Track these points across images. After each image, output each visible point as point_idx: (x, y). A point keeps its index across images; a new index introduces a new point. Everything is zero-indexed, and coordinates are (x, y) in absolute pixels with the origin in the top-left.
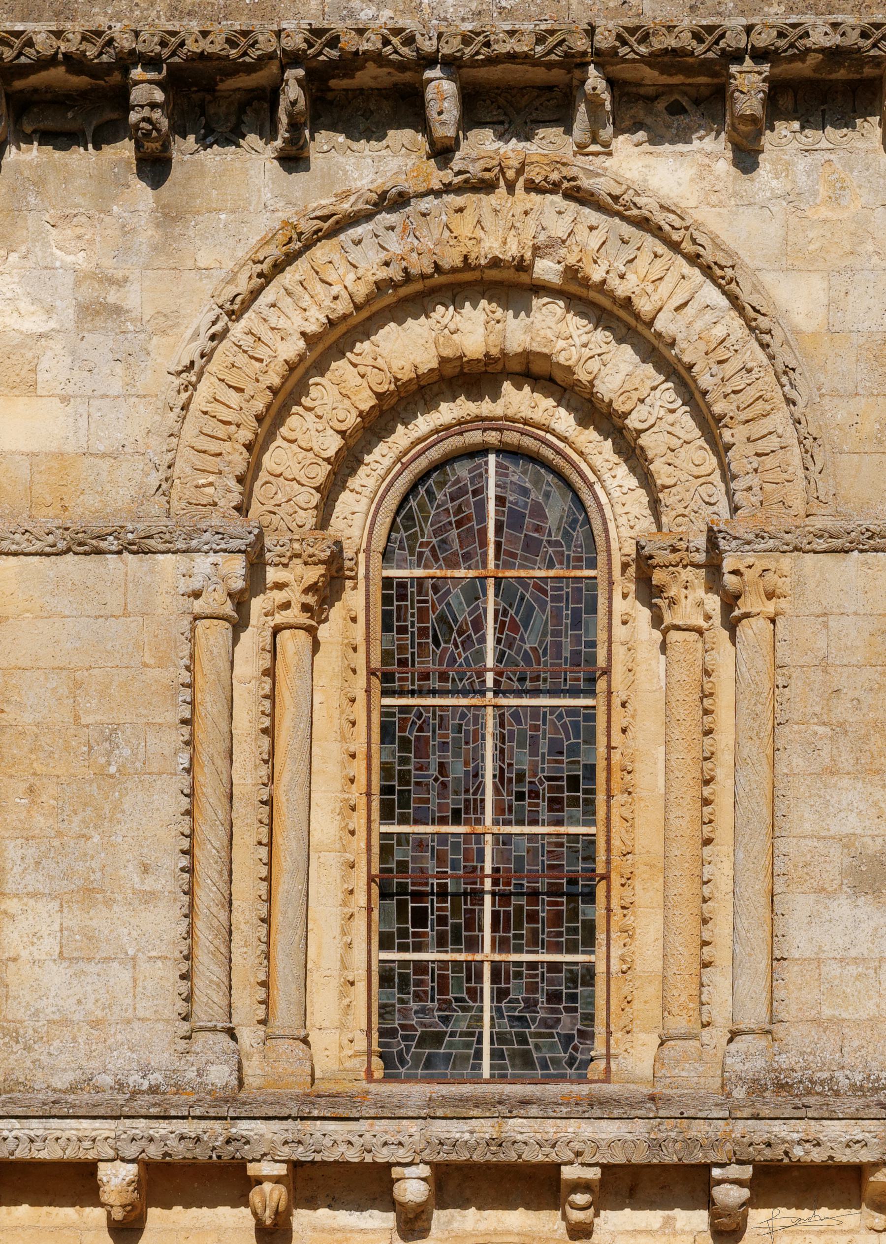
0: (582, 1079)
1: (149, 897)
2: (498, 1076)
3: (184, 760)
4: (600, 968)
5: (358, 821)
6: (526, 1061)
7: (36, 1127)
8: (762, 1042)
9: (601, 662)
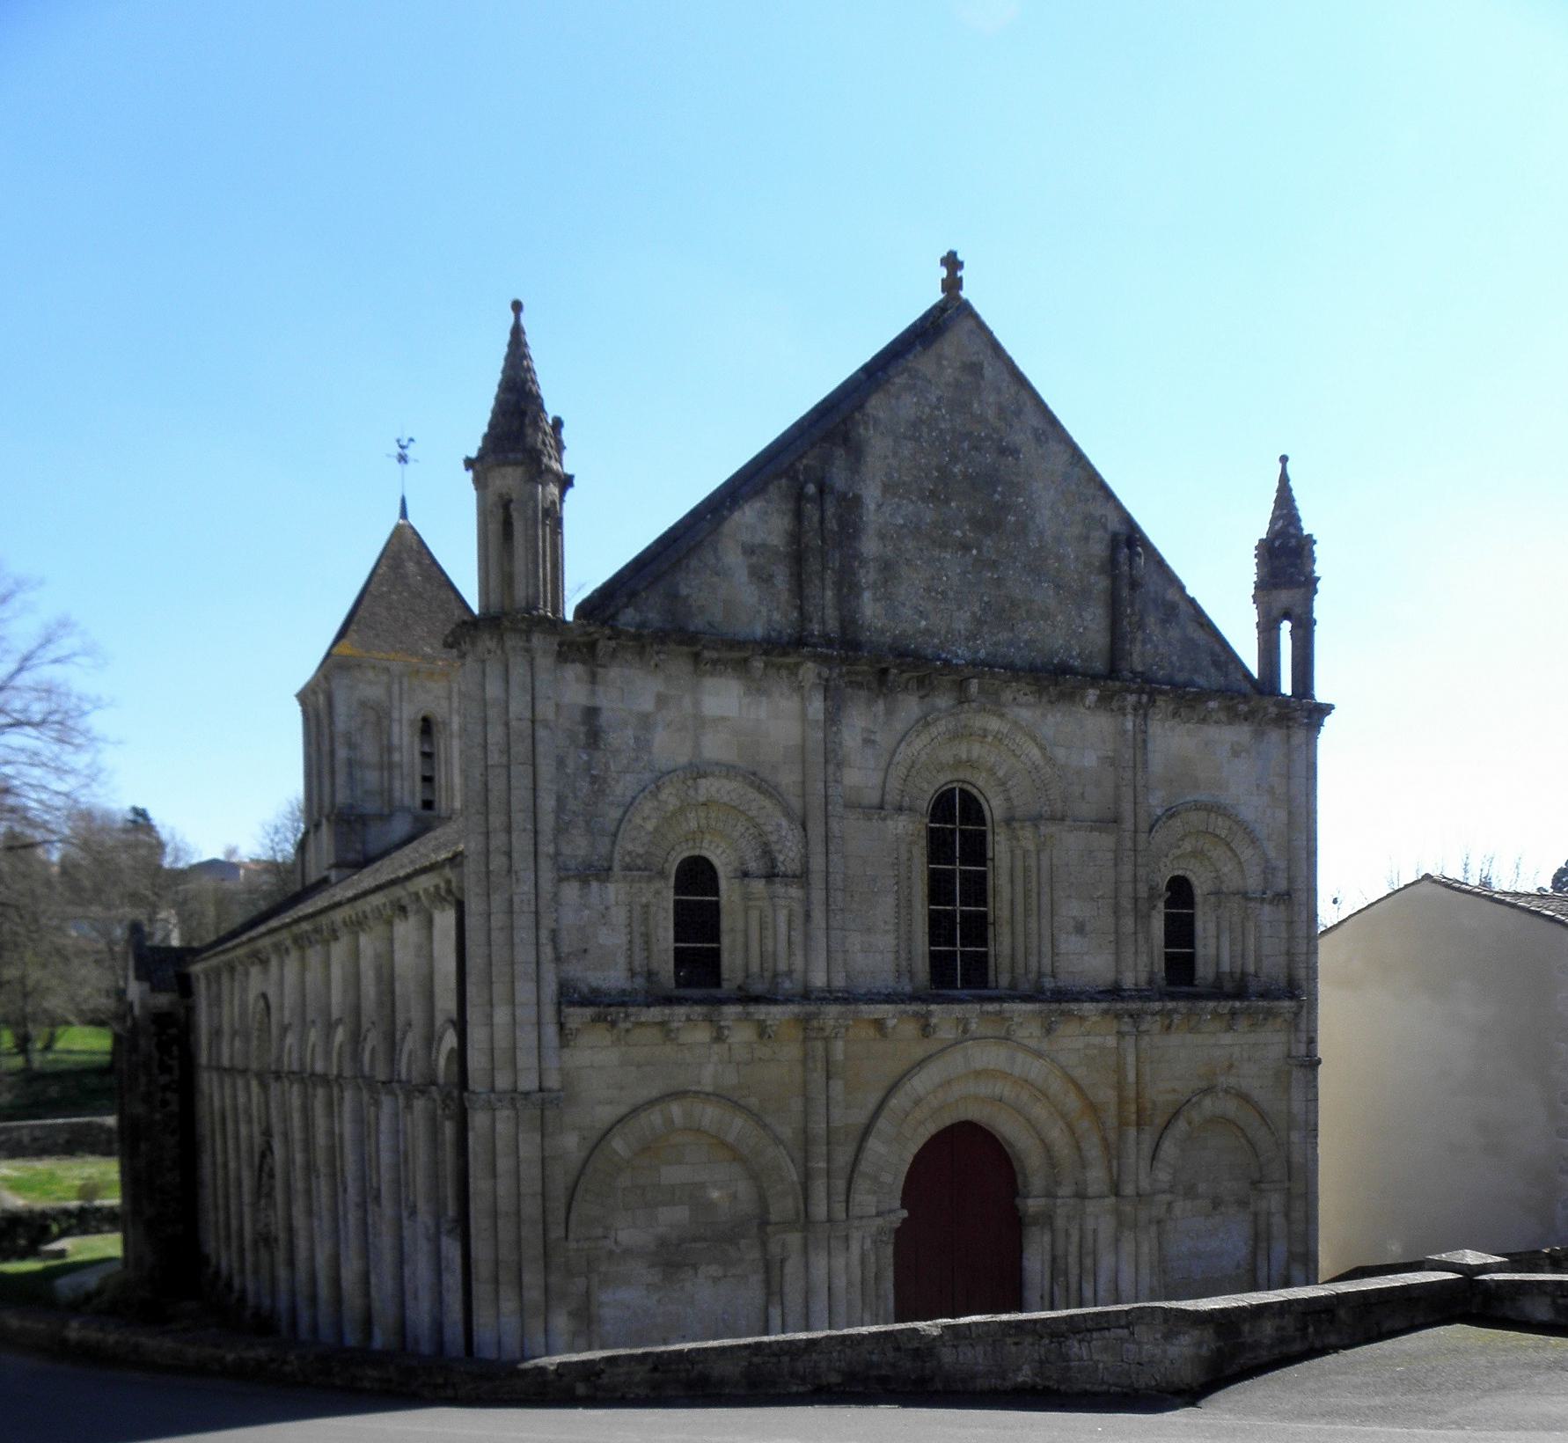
1: (887, 932)
2: (962, 988)
3: (896, 887)
4: (992, 952)
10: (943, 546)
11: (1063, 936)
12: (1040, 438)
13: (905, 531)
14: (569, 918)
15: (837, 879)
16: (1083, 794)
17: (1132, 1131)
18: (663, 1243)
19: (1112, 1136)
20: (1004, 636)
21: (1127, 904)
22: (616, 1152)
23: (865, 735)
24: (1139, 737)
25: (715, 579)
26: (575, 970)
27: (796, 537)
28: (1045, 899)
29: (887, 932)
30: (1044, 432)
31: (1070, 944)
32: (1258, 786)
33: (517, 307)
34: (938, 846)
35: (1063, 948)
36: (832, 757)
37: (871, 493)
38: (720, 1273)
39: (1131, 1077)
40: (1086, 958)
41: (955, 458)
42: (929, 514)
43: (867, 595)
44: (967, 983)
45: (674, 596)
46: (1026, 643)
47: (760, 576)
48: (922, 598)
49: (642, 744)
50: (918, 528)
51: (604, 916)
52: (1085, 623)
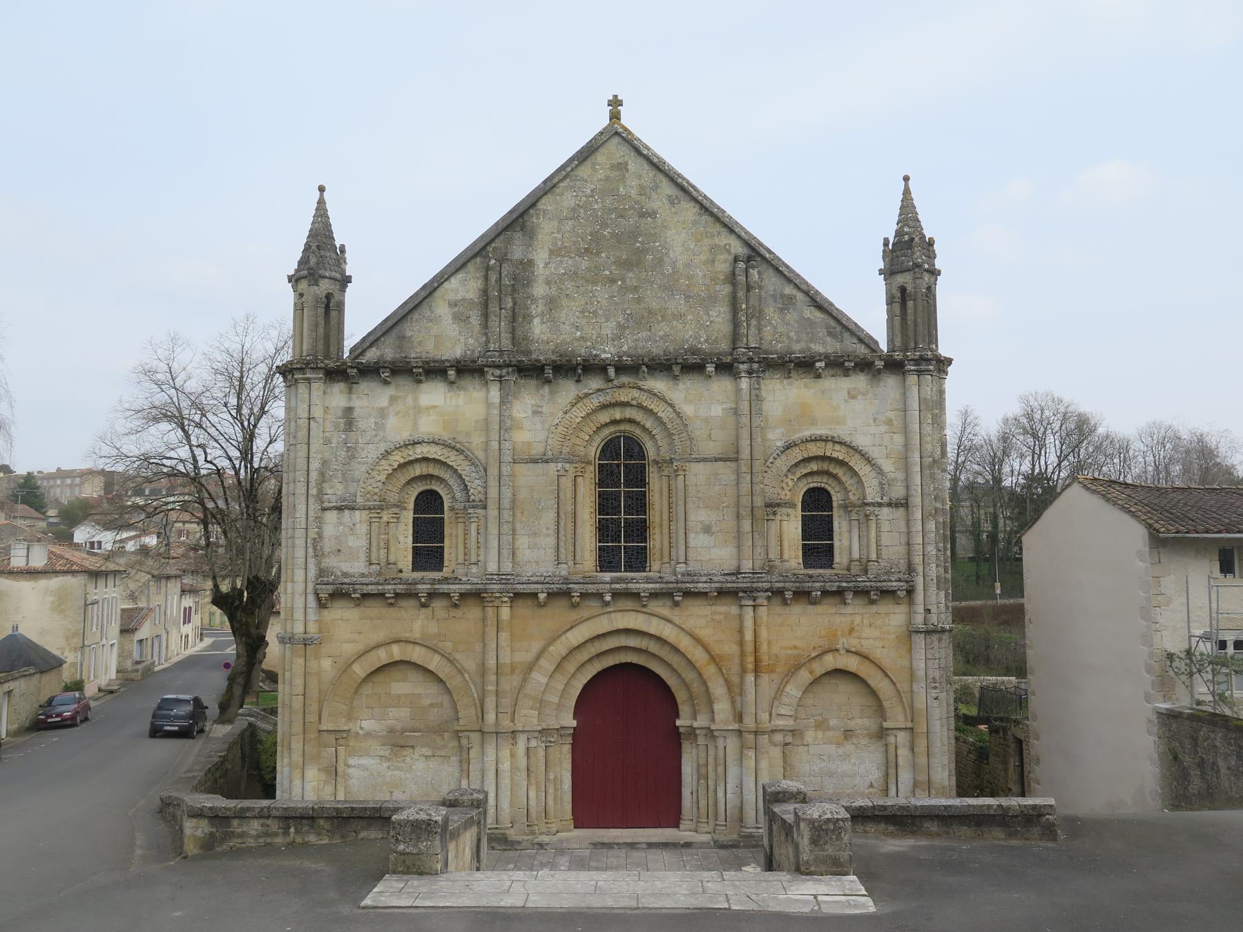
0: (644, 571)
1: (548, 535)
2: (625, 571)
5: (593, 516)
6: (631, 567)
7: (525, 586)
8: (684, 565)
9: (647, 481)
10: (595, 283)
11: (691, 536)
12: (672, 201)
13: (566, 276)
14: (329, 531)
15: (506, 503)
16: (710, 436)
17: (750, 678)
18: (391, 731)
19: (735, 680)
20: (645, 334)
21: (745, 512)
22: (355, 673)
23: (534, 409)
24: (753, 393)
25: (430, 324)
26: (330, 562)
27: (485, 292)
28: (681, 509)
29: (548, 535)
30: (677, 197)
31: (698, 540)
32: (875, 420)
33: (322, 189)
34: (606, 476)
35: (692, 543)
36: (505, 426)
37: (540, 257)
38: (430, 753)
39: (749, 636)
40: (713, 551)
41: (604, 225)
42: (584, 264)
43: (536, 321)
44: (630, 568)
45: (402, 338)
46: (661, 338)
47: (460, 318)
48: (578, 317)
49: (380, 427)
50: (575, 273)
51: (352, 529)
52: (712, 319)
